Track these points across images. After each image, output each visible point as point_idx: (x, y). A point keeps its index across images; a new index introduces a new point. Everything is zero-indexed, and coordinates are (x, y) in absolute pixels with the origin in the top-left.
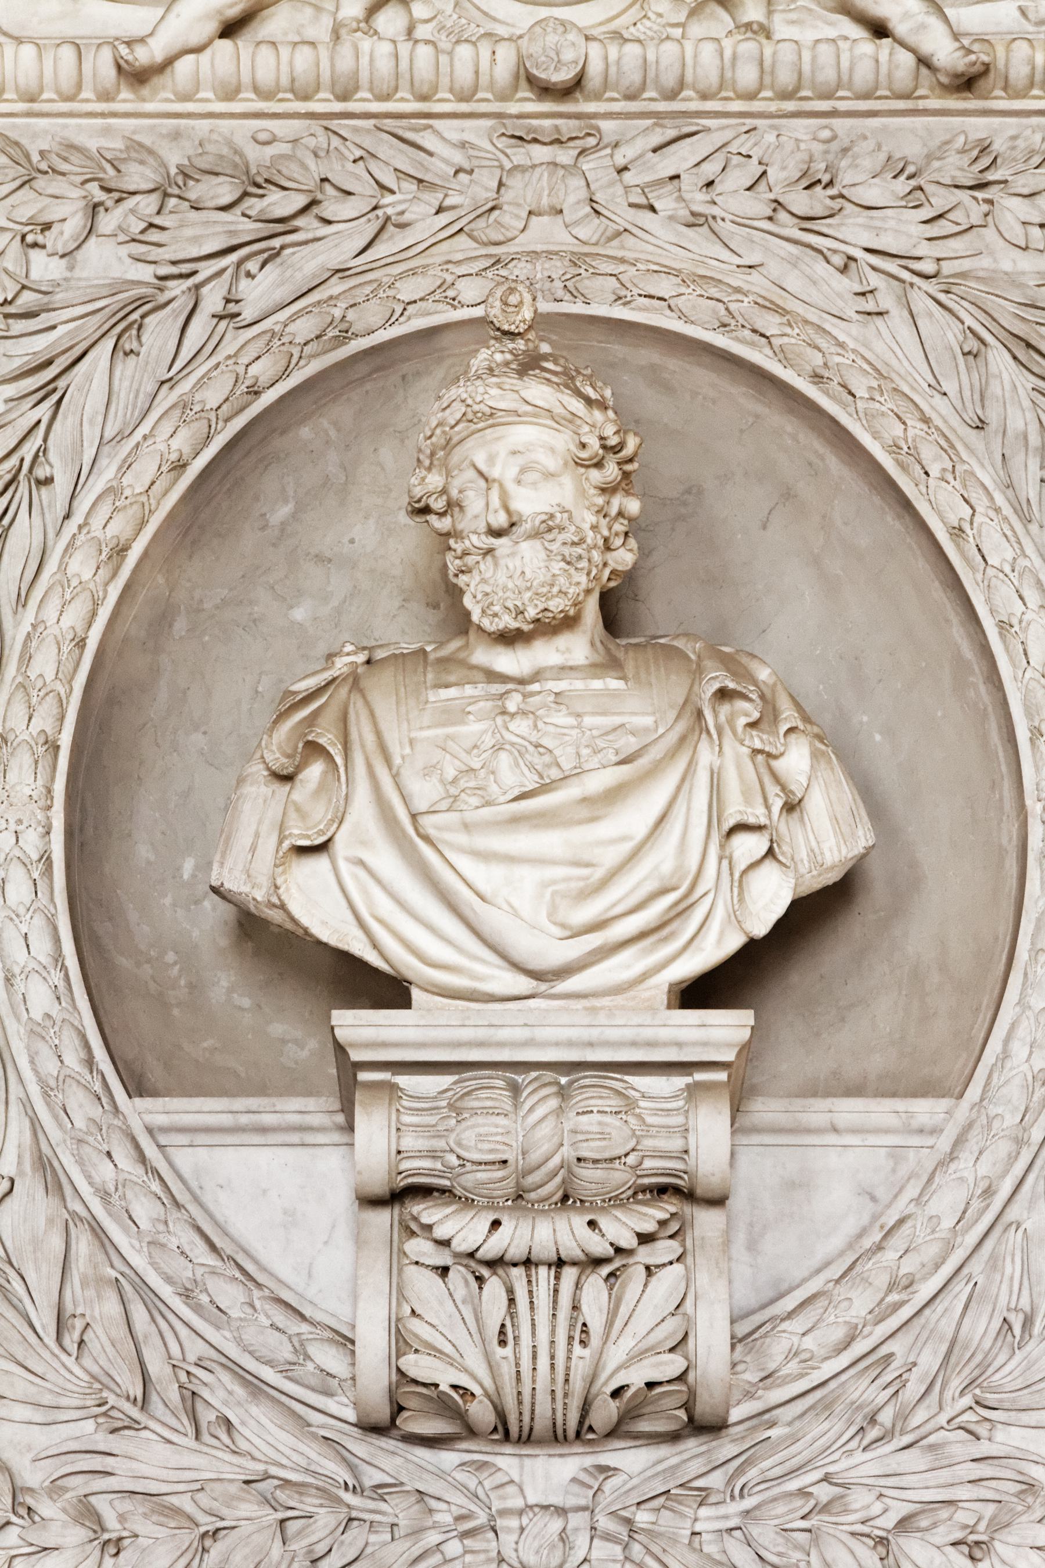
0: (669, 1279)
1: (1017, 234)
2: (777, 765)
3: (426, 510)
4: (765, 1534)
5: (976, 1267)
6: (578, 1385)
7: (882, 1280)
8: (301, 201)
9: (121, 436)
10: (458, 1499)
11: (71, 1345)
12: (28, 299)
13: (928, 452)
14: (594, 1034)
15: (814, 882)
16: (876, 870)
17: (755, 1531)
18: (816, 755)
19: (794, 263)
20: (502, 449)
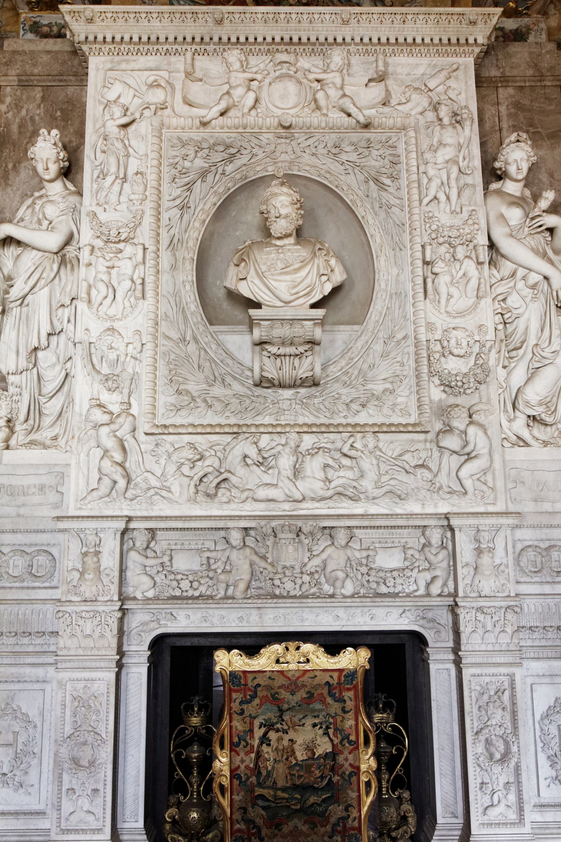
0: (310, 358)
1: (375, 158)
2: (330, 263)
3: (263, 213)
4: (326, 403)
5: (364, 356)
6: (294, 377)
7: (347, 358)
8: (237, 150)
9: (204, 198)
10: (271, 397)
11: (201, 371)
12: (184, 170)
13: (358, 202)
14: (297, 313)
15: (336, 284)
16: (347, 287)
17: (325, 403)
18: (336, 261)
19: (332, 163)
20: (278, 201)
